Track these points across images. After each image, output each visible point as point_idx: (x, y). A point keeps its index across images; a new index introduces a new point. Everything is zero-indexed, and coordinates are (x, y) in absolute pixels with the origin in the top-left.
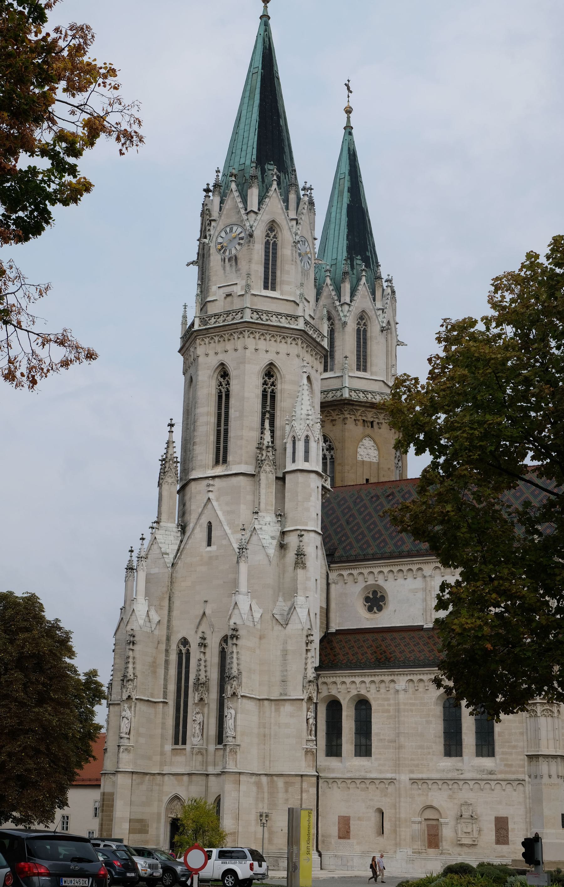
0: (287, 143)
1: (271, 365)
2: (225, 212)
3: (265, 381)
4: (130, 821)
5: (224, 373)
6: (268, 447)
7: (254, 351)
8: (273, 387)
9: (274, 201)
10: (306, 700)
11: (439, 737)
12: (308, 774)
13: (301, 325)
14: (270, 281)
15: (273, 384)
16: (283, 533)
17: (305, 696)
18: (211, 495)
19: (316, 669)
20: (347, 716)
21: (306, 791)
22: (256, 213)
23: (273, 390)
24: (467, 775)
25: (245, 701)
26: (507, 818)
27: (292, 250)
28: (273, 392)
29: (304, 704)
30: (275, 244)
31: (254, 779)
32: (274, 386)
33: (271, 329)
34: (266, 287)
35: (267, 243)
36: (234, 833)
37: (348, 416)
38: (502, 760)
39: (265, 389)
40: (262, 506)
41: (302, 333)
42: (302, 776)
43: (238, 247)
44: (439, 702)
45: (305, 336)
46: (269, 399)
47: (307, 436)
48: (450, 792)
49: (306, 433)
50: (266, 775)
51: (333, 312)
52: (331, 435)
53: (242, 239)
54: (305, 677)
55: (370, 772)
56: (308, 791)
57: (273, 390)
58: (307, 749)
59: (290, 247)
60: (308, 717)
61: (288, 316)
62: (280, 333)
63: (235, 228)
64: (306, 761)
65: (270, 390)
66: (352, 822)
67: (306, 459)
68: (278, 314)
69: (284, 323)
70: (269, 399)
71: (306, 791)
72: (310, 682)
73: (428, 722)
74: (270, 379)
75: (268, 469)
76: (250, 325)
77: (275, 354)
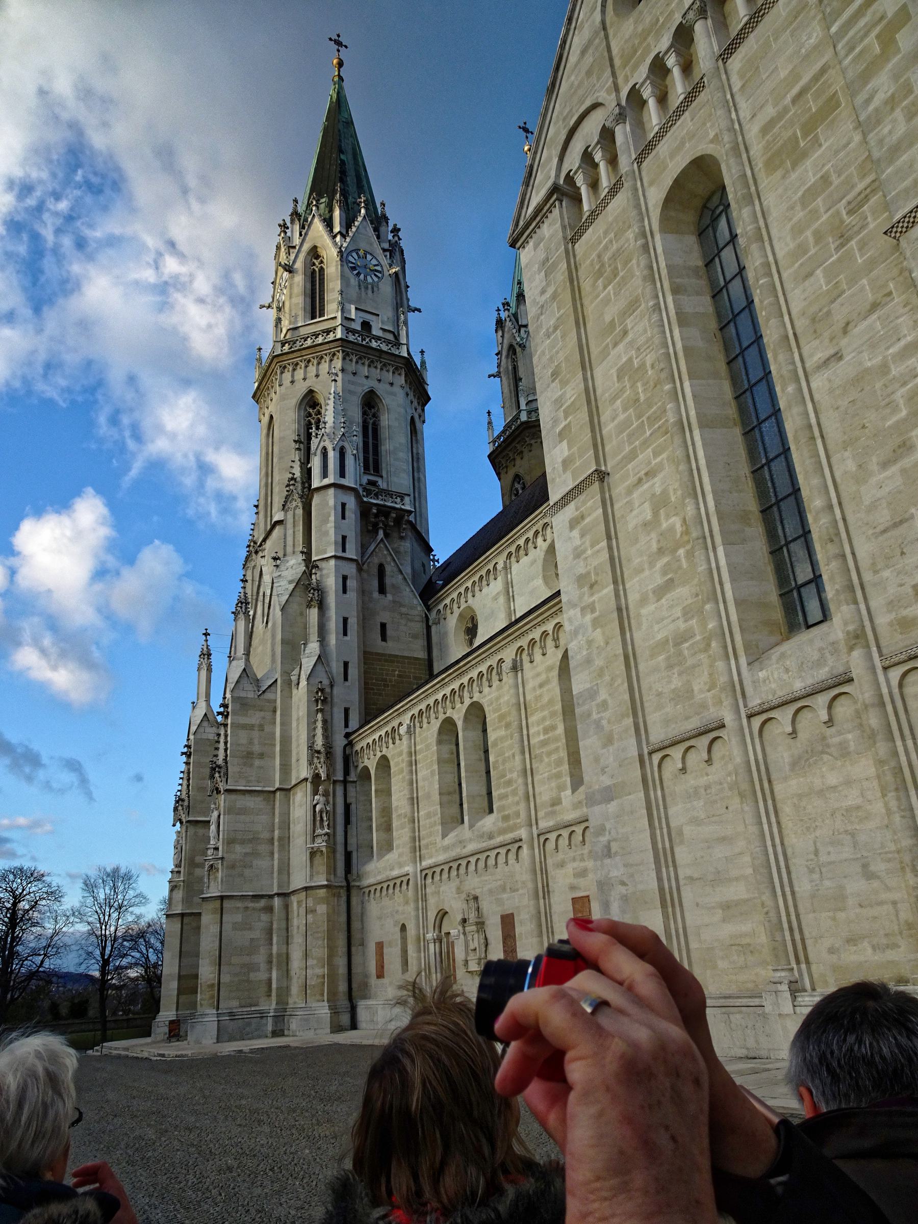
1: (311, 392)
4: (180, 977)
6: (292, 479)
7: (289, 384)
9: (318, 226)
10: (310, 780)
11: (449, 793)
12: (313, 884)
13: (339, 336)
14: (315, 306)
15: (319, 413)
16: (308, 574)
17: (310, 776)
18: (263, 562)
19: (347, 735)
20: (376, 791)
21: (312, 911)
22: (294, 247)
24: (471, 847)
25: (233, 797)
26: (512, 914)
27: (337, 265)
29: (309, 784)
31: (263, 903)
33: (304, 352)
34: (313, 317)
36: (212, 985)
37: (533, 442)
38: (499, 811)
40: (289, 549)
41: (339, 343)
42: (306, 889)
44: (445, 737)
45: (345, 344)
47: (325, 448)
48: (455, 883)
49: (322, 444)
50: (279, 895)
51: (514, 343)
52: (521, 472)
54: (311, 747)
55: (392, 869)
56: (313, 911)
58: (312, 848)
59: (334, 263)
60: (315, 802)
61: (323, 331)
64: (312, 866)
66: (385, 950)
67: (325, 475)
68: (316, 335)
69: (320, 340)
71: (312, 911)
72: (318, 752)
73: (432, 773)
75: (294, 504)
76: (281, 359)
77: (314, 379)
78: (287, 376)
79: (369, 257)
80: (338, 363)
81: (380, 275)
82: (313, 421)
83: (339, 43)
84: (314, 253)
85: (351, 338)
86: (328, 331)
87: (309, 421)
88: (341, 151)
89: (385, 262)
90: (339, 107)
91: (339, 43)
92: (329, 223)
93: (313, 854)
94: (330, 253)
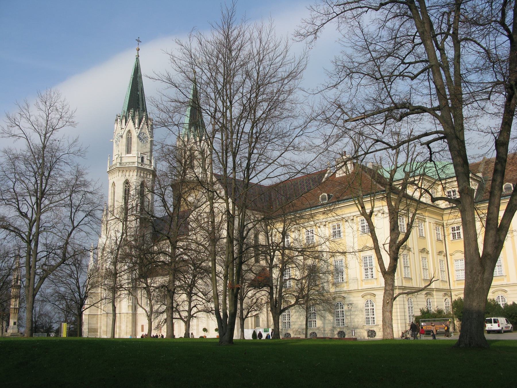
0: (141, 99)
5: (114, 184)
9: (131, 123)
13: (136, 165)
14: (128, 150)
30: (131, 137)
34: (128, 153)
62: (129, 169)
78: (120, 173)
80: (135, 173)
83: (139, 41)
84: (129, 131)
85: (140, 166)
86: (133, 163)
88: (138, 91)
89: (149, 136)
90: (137, 70)
91: (139, 41)
92: (134, 124)
93: (128, 306)
94: (135, 134)
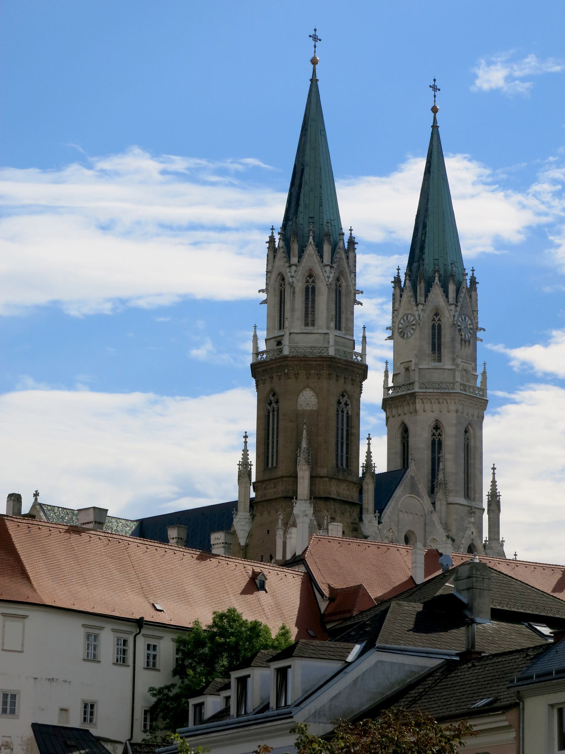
2: (402, 304)
3: (434, 433)
8: (439, 437)
23: (439, 439)
28: (440, 440)
30: (440, 326)
32: (441, 436)
35: (434, 326)
39: (434, 439)
43: (412, 331)
46: (436, 446)
53: (413, 325)
57: (439, 439)
63: (409, 316)
65: (437, 440)
70: (436, 446)
74: (437, 431)
79: (467, 319)
81: (471, 331)
82: (437, 440)
87: (434, 439)
